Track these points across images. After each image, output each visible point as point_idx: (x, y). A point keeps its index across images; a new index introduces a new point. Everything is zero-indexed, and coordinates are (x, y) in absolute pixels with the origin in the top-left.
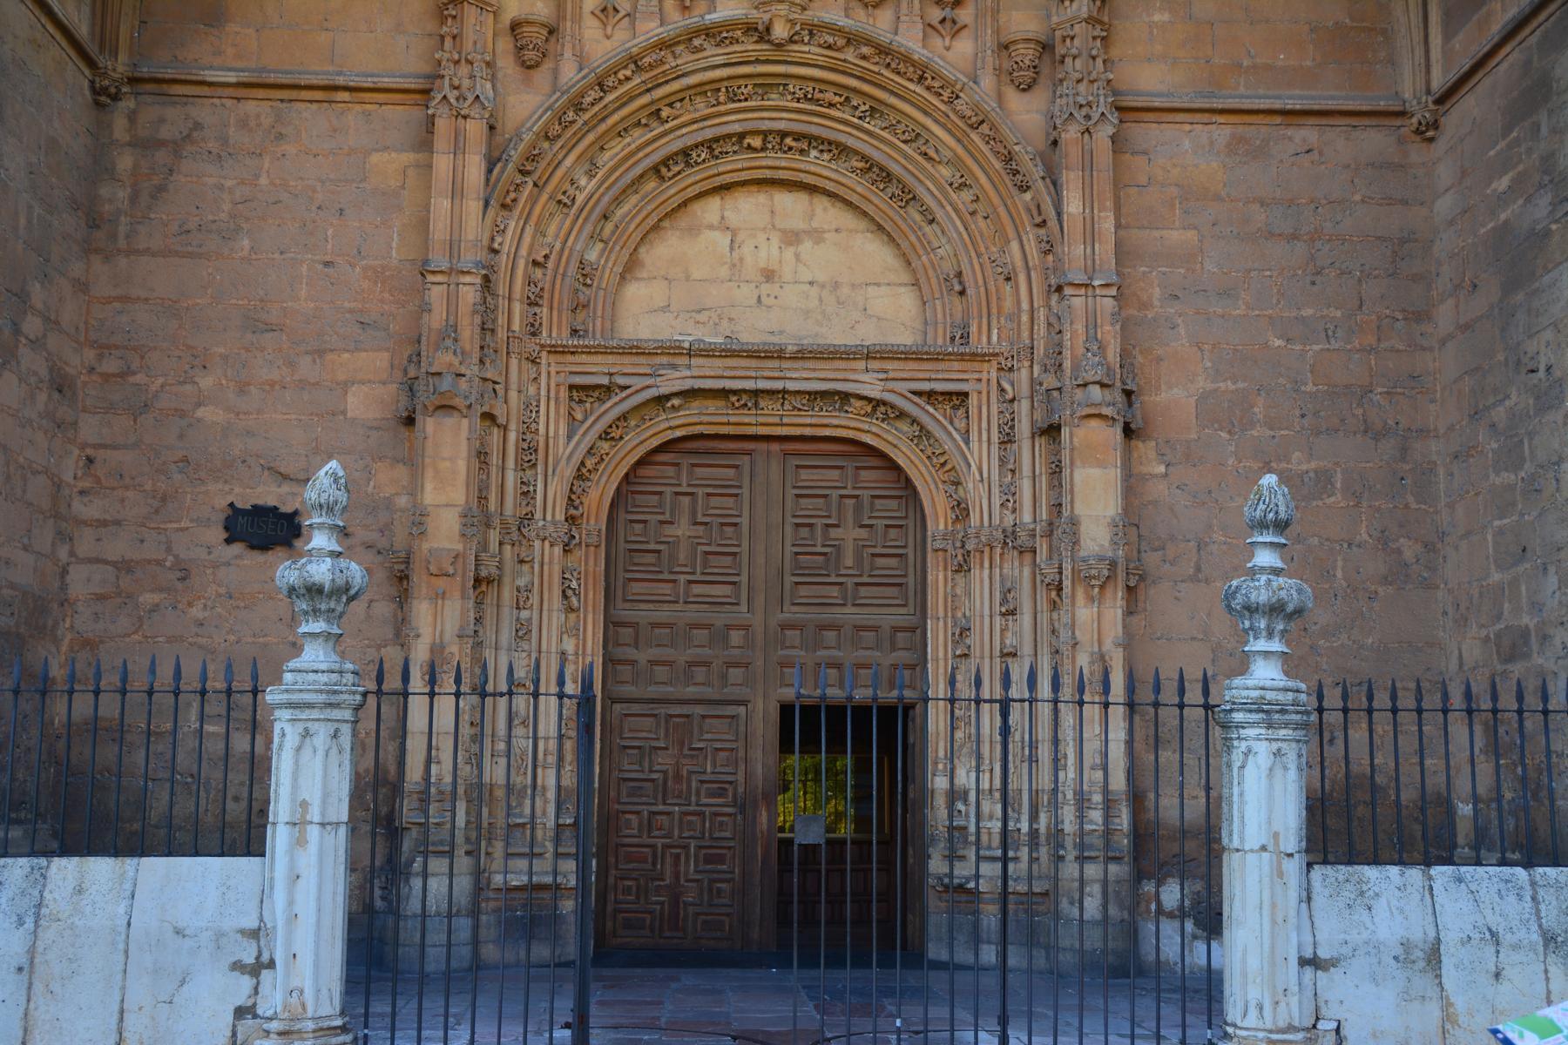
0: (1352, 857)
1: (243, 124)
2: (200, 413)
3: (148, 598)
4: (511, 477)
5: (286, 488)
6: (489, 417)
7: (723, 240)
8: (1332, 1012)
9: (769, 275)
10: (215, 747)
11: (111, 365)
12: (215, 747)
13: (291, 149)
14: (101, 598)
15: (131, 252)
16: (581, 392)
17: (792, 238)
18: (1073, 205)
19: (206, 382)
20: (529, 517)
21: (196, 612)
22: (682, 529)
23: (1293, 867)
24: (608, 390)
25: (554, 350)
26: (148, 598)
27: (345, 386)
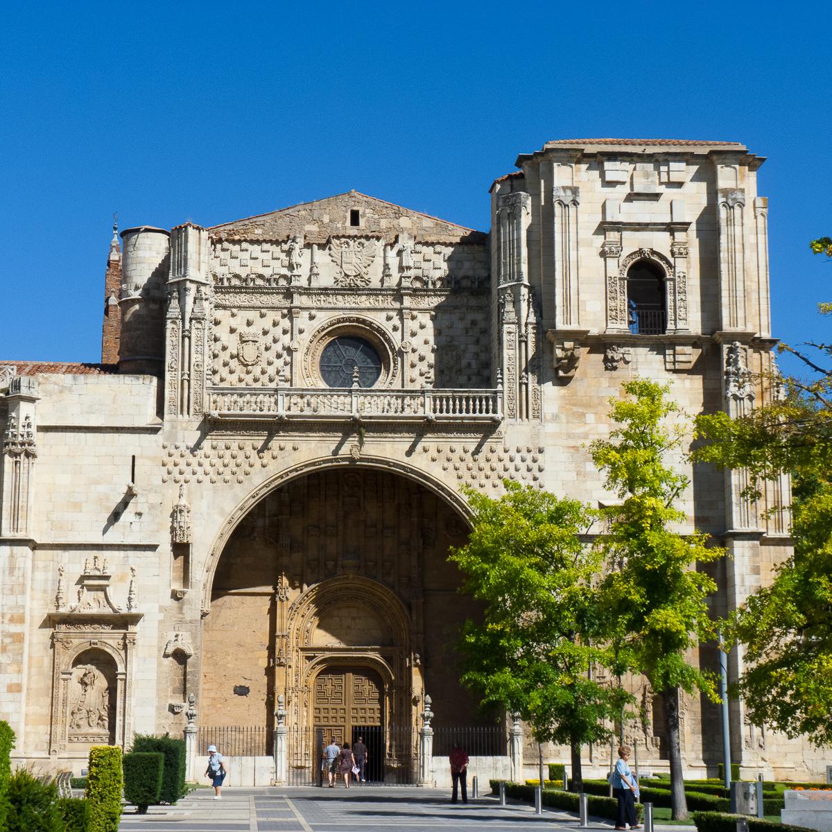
0: (437, 755)
1: (235, 601)
2: (229, 665)
3: (219, 706)
4: (294, 678)
5: (246, 681)
6: (290, 667)
7: (338, 619)
8: (435, 779)
9: (349, 627)
10: (233, 737)
11: (209, 655)
12: (233, 737)
13: (245, 606)
14: (209, 706)
15: (213, 630)
16: (307, 658)
17: (354, 619)
18: (414, 618)
19: (229, 658)
20: (297, 686)
21: (229, 708)
22: (330, 686)
23: (431, 756)
24: (315, 657)
25: (302, 649)
26: (219, 706)
27: (258, 658)
